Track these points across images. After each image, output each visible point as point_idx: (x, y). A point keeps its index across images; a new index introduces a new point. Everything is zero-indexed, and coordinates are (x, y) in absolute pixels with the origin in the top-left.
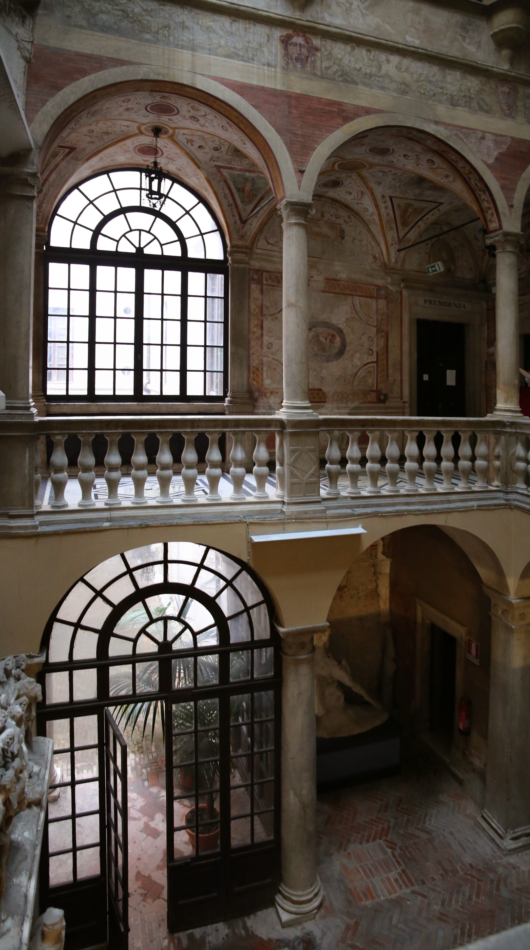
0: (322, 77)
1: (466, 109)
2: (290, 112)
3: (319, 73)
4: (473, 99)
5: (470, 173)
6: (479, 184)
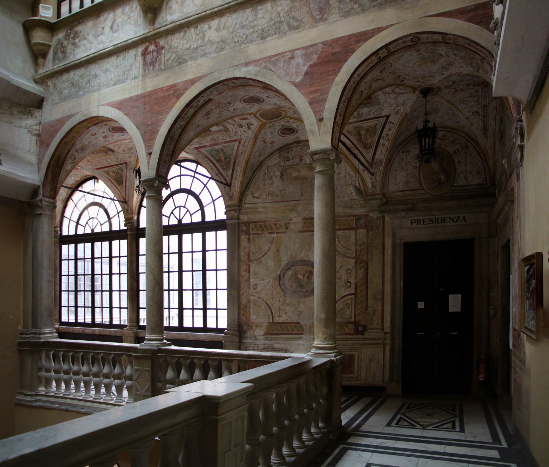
0: (165, 70)
1: (276, 36)
2: (145, 109)
3: (163, 67)
4: (283, 22)
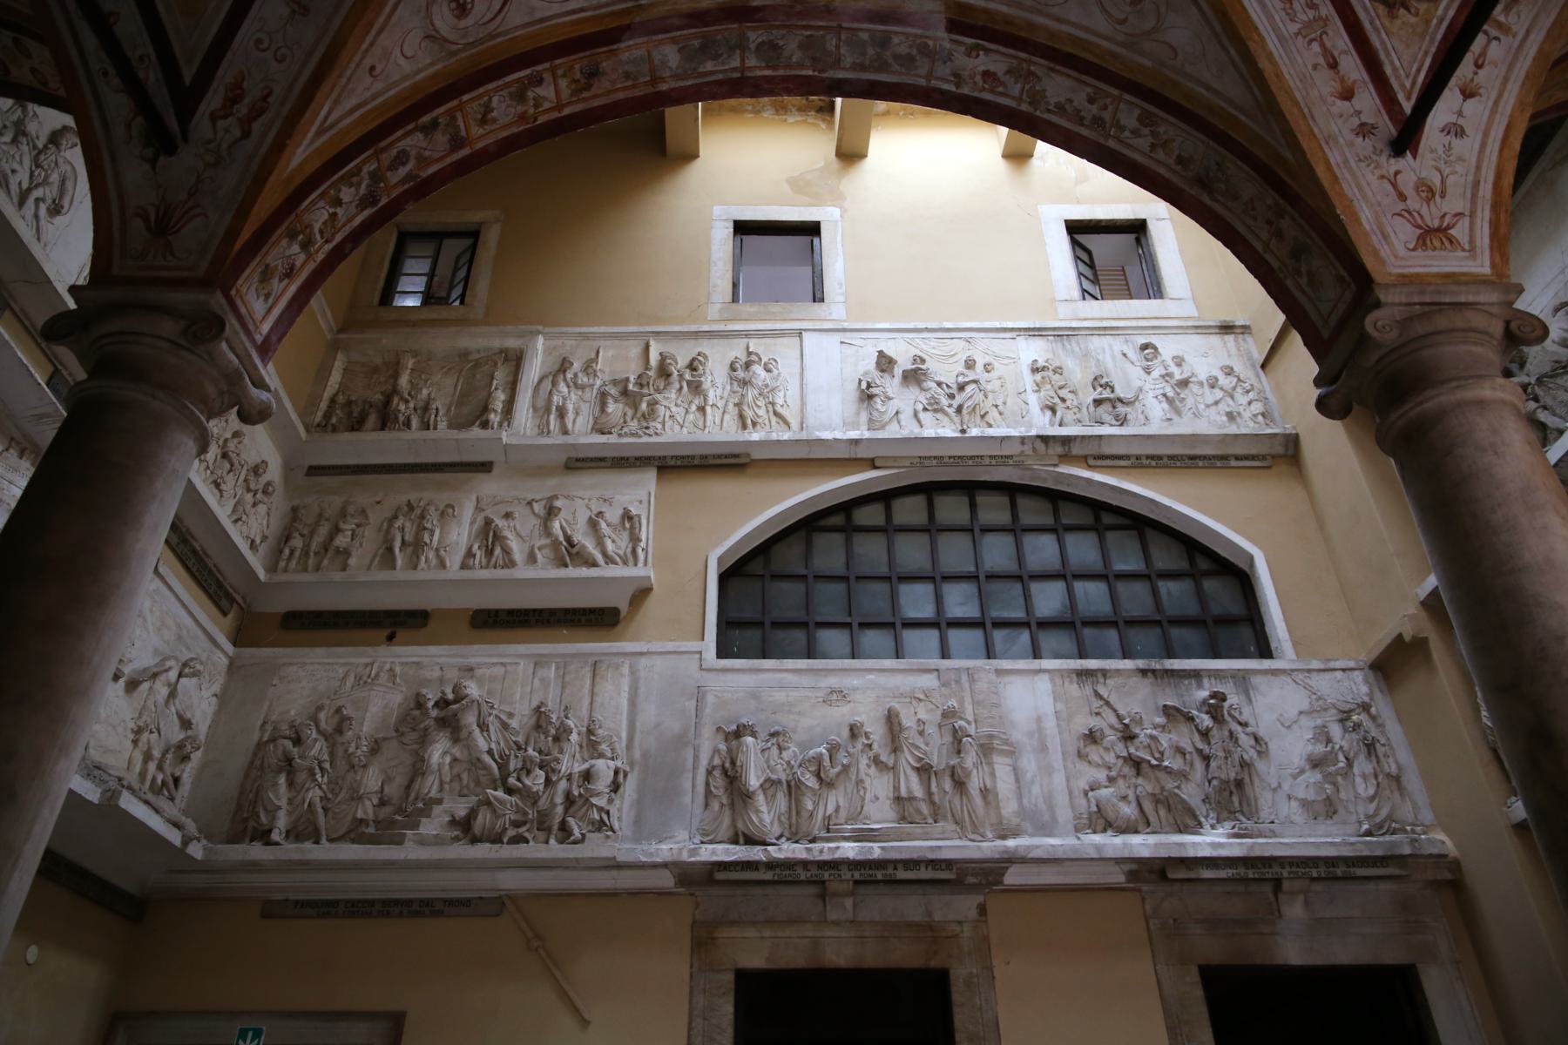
5: (457, 142)
6: (403, 171)
